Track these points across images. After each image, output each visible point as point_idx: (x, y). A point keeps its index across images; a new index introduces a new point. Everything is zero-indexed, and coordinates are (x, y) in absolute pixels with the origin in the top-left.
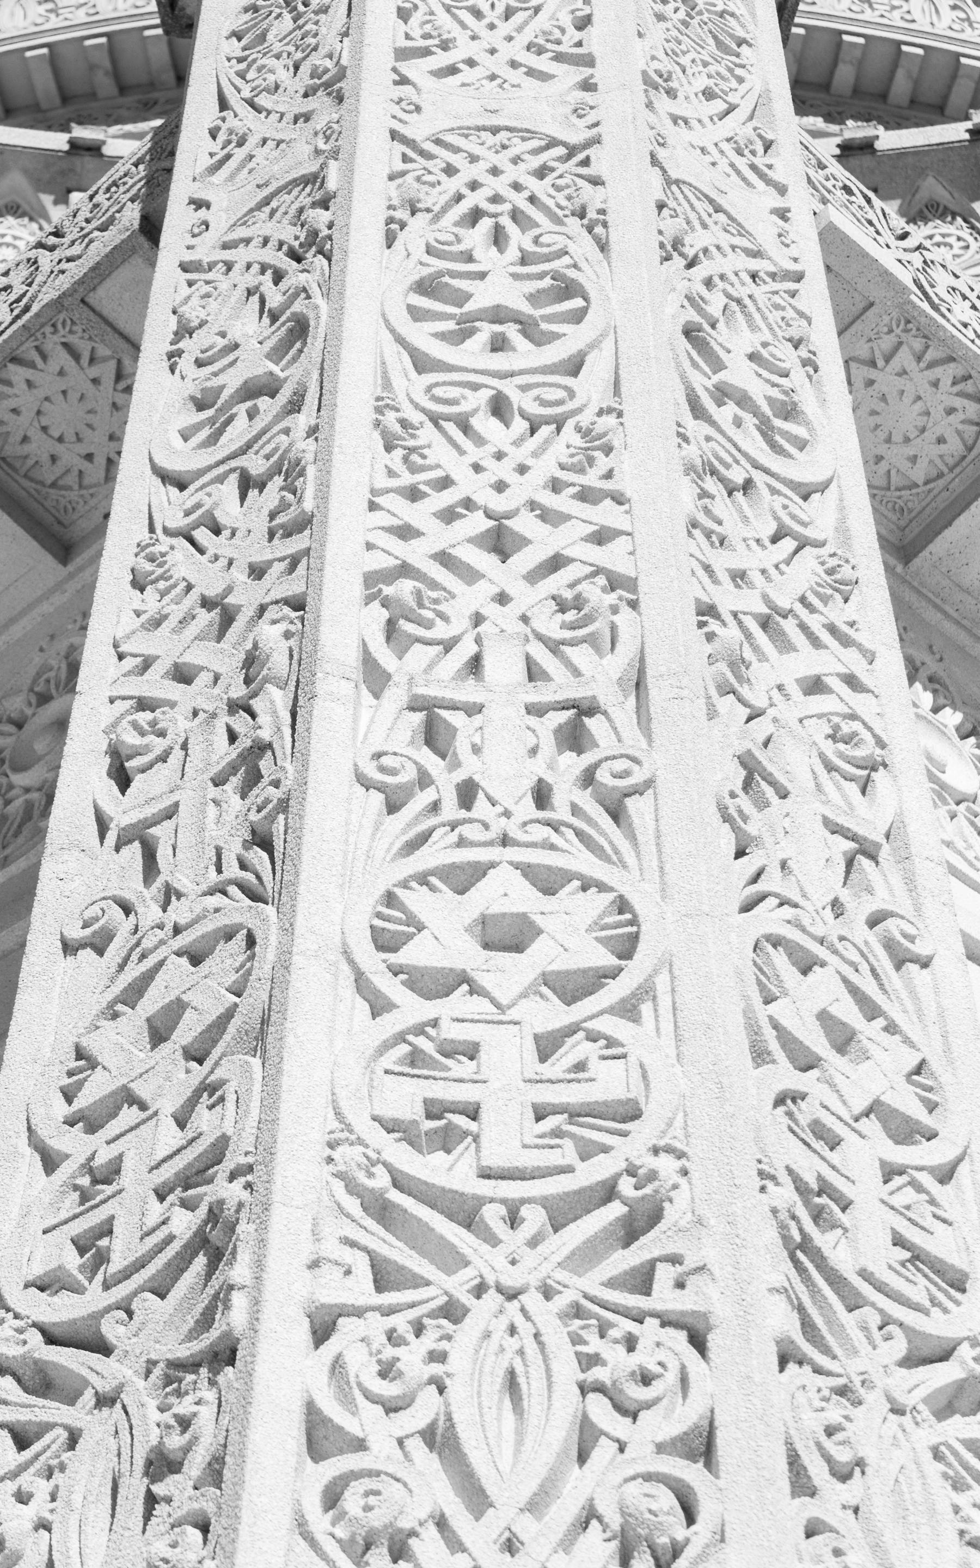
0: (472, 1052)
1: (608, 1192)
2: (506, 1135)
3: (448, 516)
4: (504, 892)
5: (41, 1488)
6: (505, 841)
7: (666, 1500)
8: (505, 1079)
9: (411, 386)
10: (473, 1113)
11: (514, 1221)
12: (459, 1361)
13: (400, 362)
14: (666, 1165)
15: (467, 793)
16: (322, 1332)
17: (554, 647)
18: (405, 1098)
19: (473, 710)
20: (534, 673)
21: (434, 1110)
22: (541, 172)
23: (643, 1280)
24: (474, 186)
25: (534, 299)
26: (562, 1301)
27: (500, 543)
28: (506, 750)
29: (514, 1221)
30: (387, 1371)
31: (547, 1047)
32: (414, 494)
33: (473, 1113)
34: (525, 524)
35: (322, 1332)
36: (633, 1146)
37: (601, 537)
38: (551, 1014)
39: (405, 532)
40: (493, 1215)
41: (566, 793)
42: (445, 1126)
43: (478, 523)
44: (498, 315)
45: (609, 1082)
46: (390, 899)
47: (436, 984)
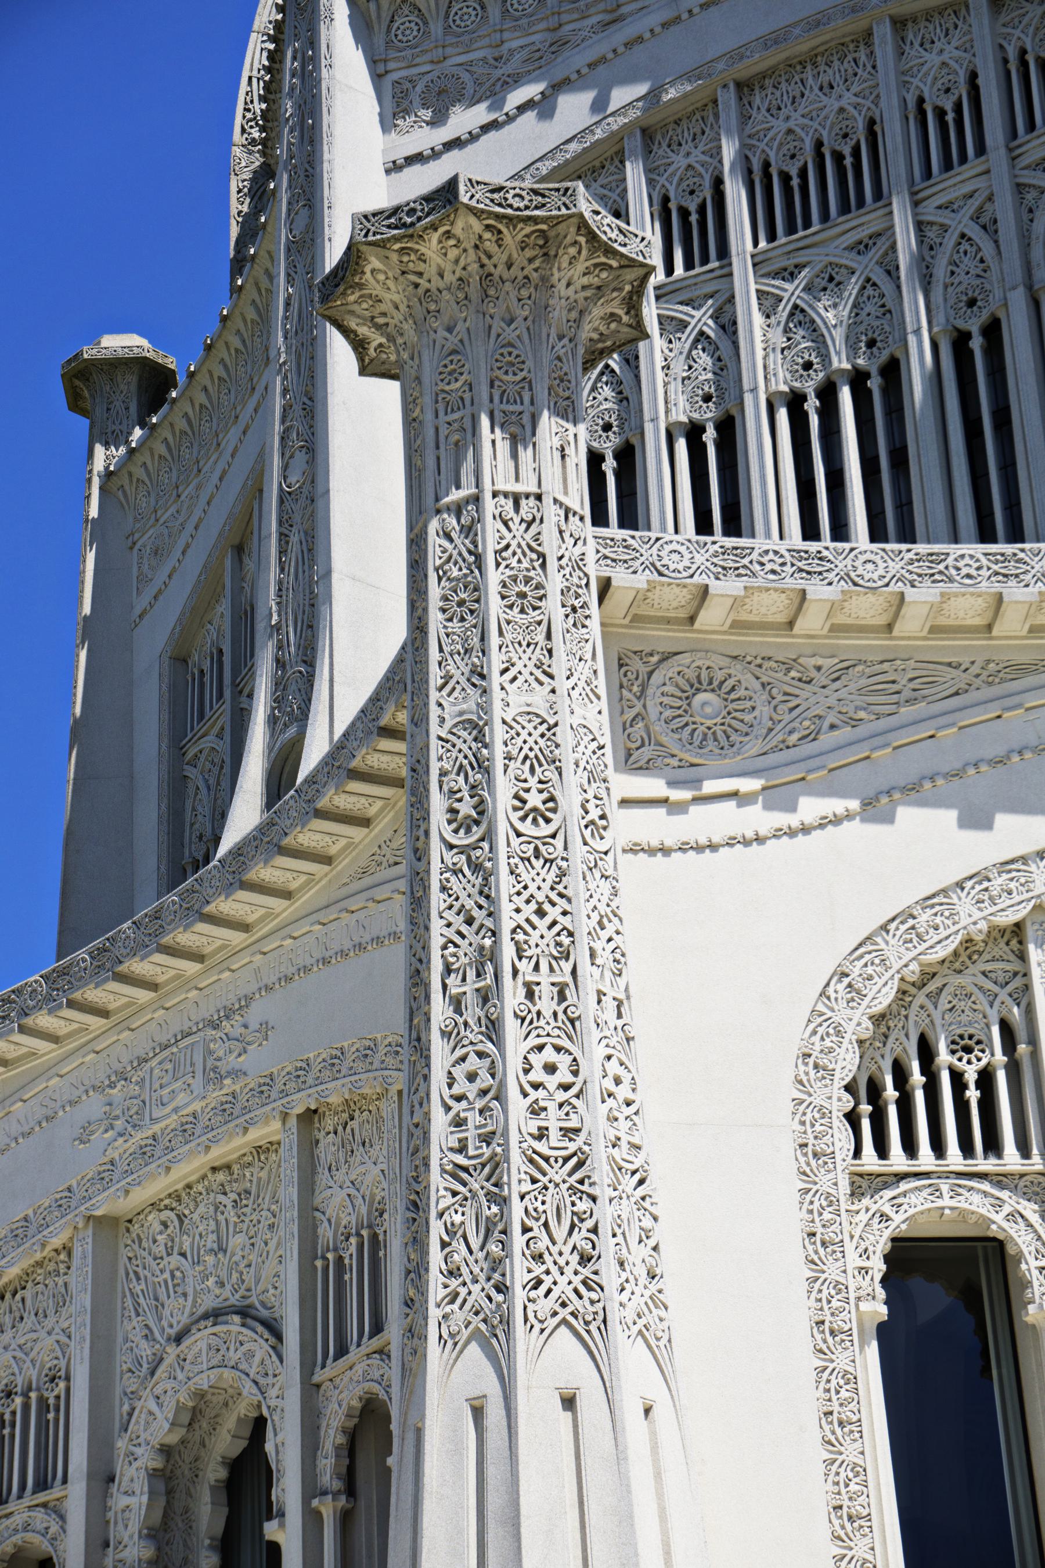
0: (545, 1109)
1: (575, 1154)
2: (554, 1135)
3: (528, 902)
4: (549, 1055)
5: (460, 1210)
6: (548, 1035)
7: (590, 1245)
8: (553, 1120)
9: (515, 841)
10: (547, 1129)
11: (556, 1161)
12: (548, 1199)
13: (512, 834)
14: (586, 1148)
15: (539, 1013)
16: (522, 1198)
17: (555, 958)
18: (533, 1126)
19: (538, 984)
20: (552, 969)
21: (540, 1128)
22: (542, 736)
23: (581, 1182)
24: (525, 742)
25: (544, 803)
26: (567, 1185)
27: (541, 913)
28: (546, 1004)
29: (556, 1161)
30: (535, 1210)
31: (561, 1106)
32: (519, 894)
33: (547, 1129)
34: (547, 907)
35: (522, 1198)
36: (580, 1140)
37: (565, 913)
38: (561, 1096)
39: (518, 911)
40: (552, 1160)
41: (561, 1016)
42: (542, 1134)
43: (533, 906)
44: (535, 809)
45: (573, 1123)
46: (525, 1058)
47: (536, 1086)
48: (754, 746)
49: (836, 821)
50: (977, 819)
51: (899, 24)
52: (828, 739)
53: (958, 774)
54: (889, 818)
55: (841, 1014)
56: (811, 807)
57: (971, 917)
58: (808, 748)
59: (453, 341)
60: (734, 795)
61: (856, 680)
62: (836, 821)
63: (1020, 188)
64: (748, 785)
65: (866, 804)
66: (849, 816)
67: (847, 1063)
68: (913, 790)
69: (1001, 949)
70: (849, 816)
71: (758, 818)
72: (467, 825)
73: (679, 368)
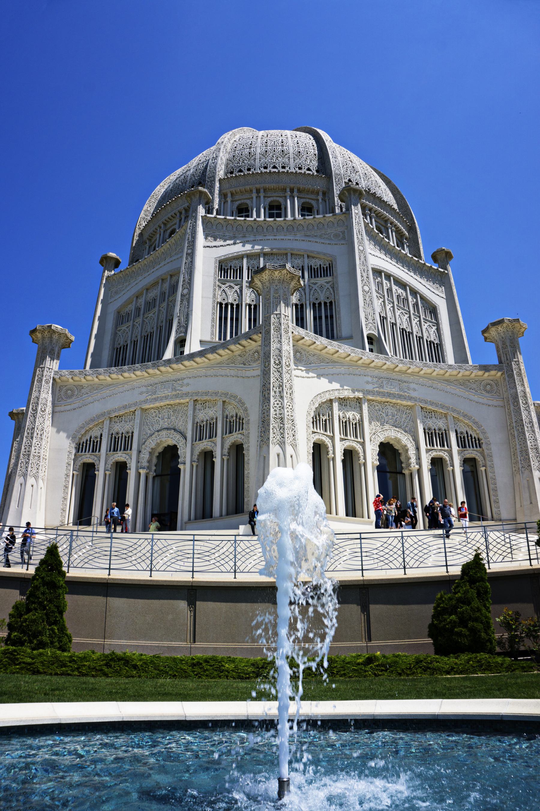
48: (303, 363)
49: (313, 377)
50: (330, 382)
51: (292, 254)
52: (312, 365)
53: (327, 375)
54: (320, 379)
55: (312, 407)
56: (311, 374)
57: (328, 397)
58: (310, 365)
59: (276, 288)
60: (301, 370)
61: (315, 357)
62: (313, 377)
63: (309, 286)
64: (303, 369)
65: (317, 376)
66: (314, 377)
67: (312, 414)
68: (322, 375)
69: (329, 403)
70: (314, 377)
71: (304, 374)
72: (277, 365)
73: (248, 294)
